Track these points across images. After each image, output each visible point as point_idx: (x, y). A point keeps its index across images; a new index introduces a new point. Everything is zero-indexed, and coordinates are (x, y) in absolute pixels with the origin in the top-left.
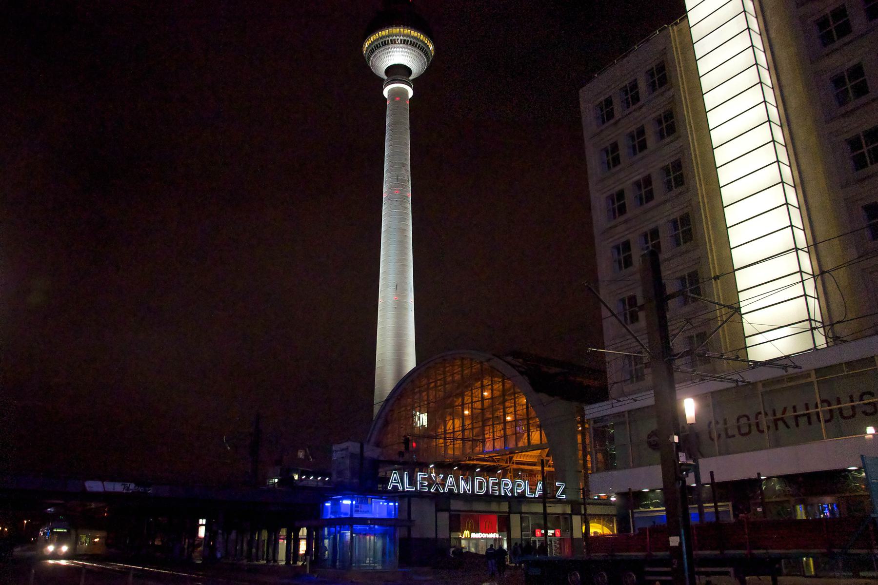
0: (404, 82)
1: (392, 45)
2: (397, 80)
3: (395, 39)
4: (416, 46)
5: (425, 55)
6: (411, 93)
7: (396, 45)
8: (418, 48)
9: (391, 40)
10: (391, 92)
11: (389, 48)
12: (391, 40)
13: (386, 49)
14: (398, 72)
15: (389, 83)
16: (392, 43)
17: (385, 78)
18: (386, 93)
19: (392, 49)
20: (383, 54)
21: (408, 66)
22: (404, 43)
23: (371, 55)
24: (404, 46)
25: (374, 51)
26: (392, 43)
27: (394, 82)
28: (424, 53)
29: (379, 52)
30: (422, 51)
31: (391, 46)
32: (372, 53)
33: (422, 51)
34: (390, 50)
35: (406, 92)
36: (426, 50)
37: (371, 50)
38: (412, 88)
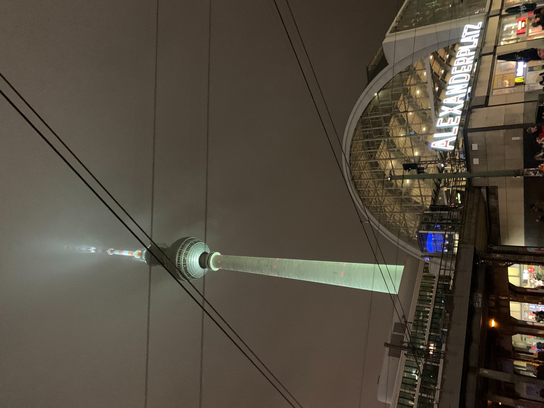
0: (210, 257)
1: (187, 262)
2: (208, 260)
3: (184, 260)
4: (190, 248)
5: (196, 243)
6: (218, 254)
7: (187, 260)
8: (191, 246)
9: (183, 262)
10: (216, 265)
11: (188, 264)
12: (183, 262)
13: (188, 266)
14: (204, 261)
15: (209, 266)
16: (185, 262)
17: (207, 269)
18: (215, 269)
19: (189, 262)
20: (191, 268)
21: (200, 255)
22: (186, 254)
23: (191, 276)
24: (188, 254)
25: (189, 274)
26: (185, 262)
27: (209, 263)
28: (195, 243)
29: (190, 271)
30: (193, 244)
31: (187, 263)
32: (190, 275)
33: (193, 244)
34: (189, 264)
35: (217, 256)
36: (193, 242)
37: (188, 276)
38: (214, 253)
